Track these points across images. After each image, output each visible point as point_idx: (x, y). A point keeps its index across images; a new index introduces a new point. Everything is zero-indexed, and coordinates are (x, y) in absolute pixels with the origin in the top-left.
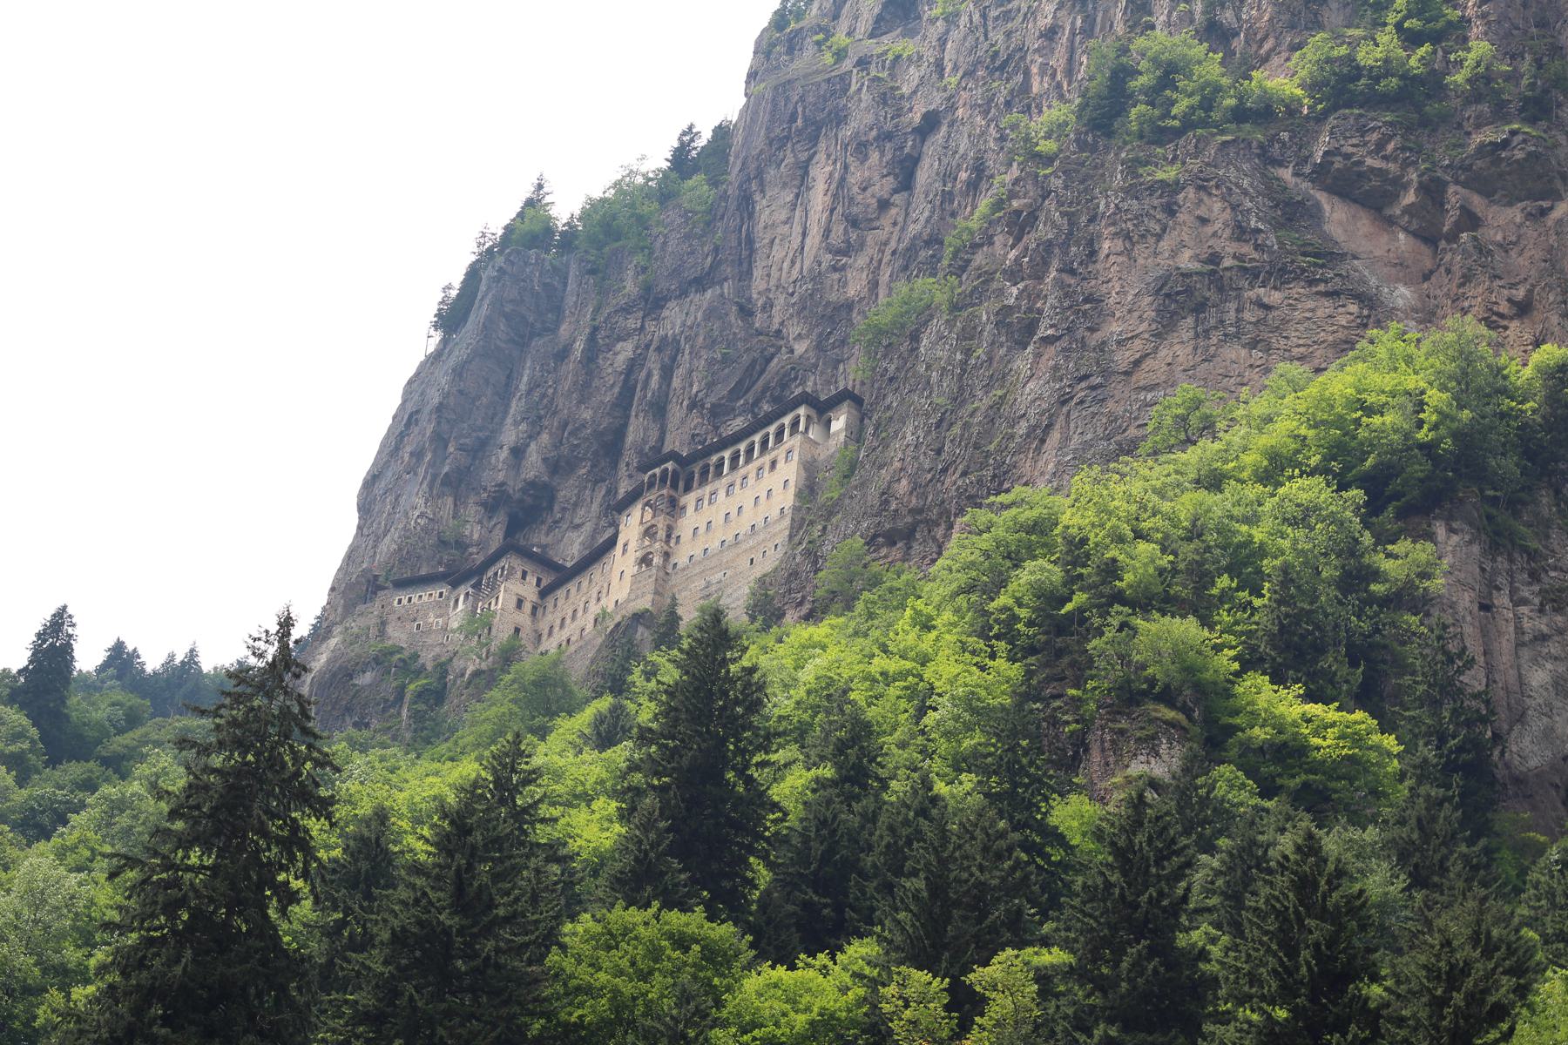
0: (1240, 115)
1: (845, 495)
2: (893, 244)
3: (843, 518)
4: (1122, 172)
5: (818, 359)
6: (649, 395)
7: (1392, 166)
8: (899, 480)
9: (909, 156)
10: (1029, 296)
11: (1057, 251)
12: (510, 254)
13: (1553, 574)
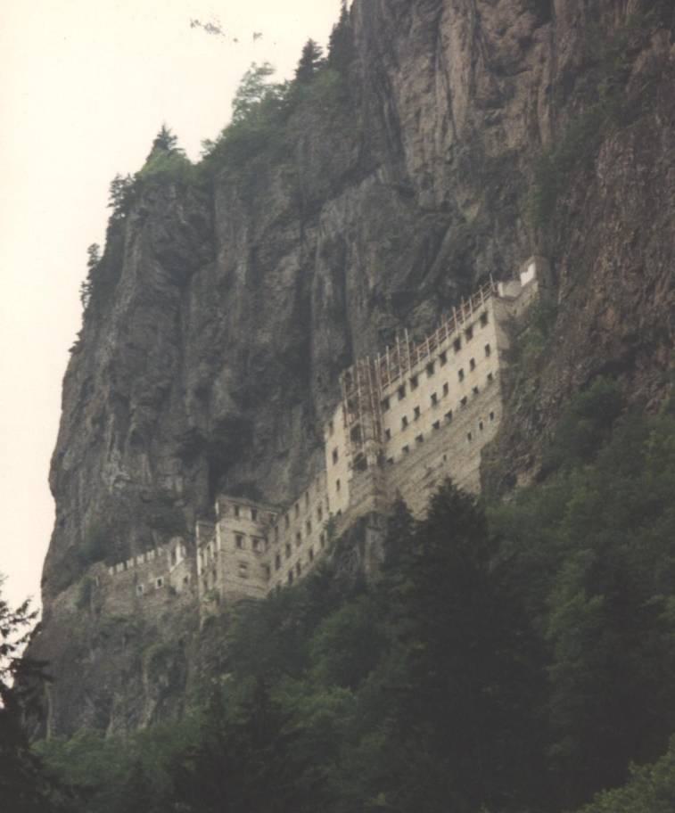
6: (326, 303)
8: (605, 312)
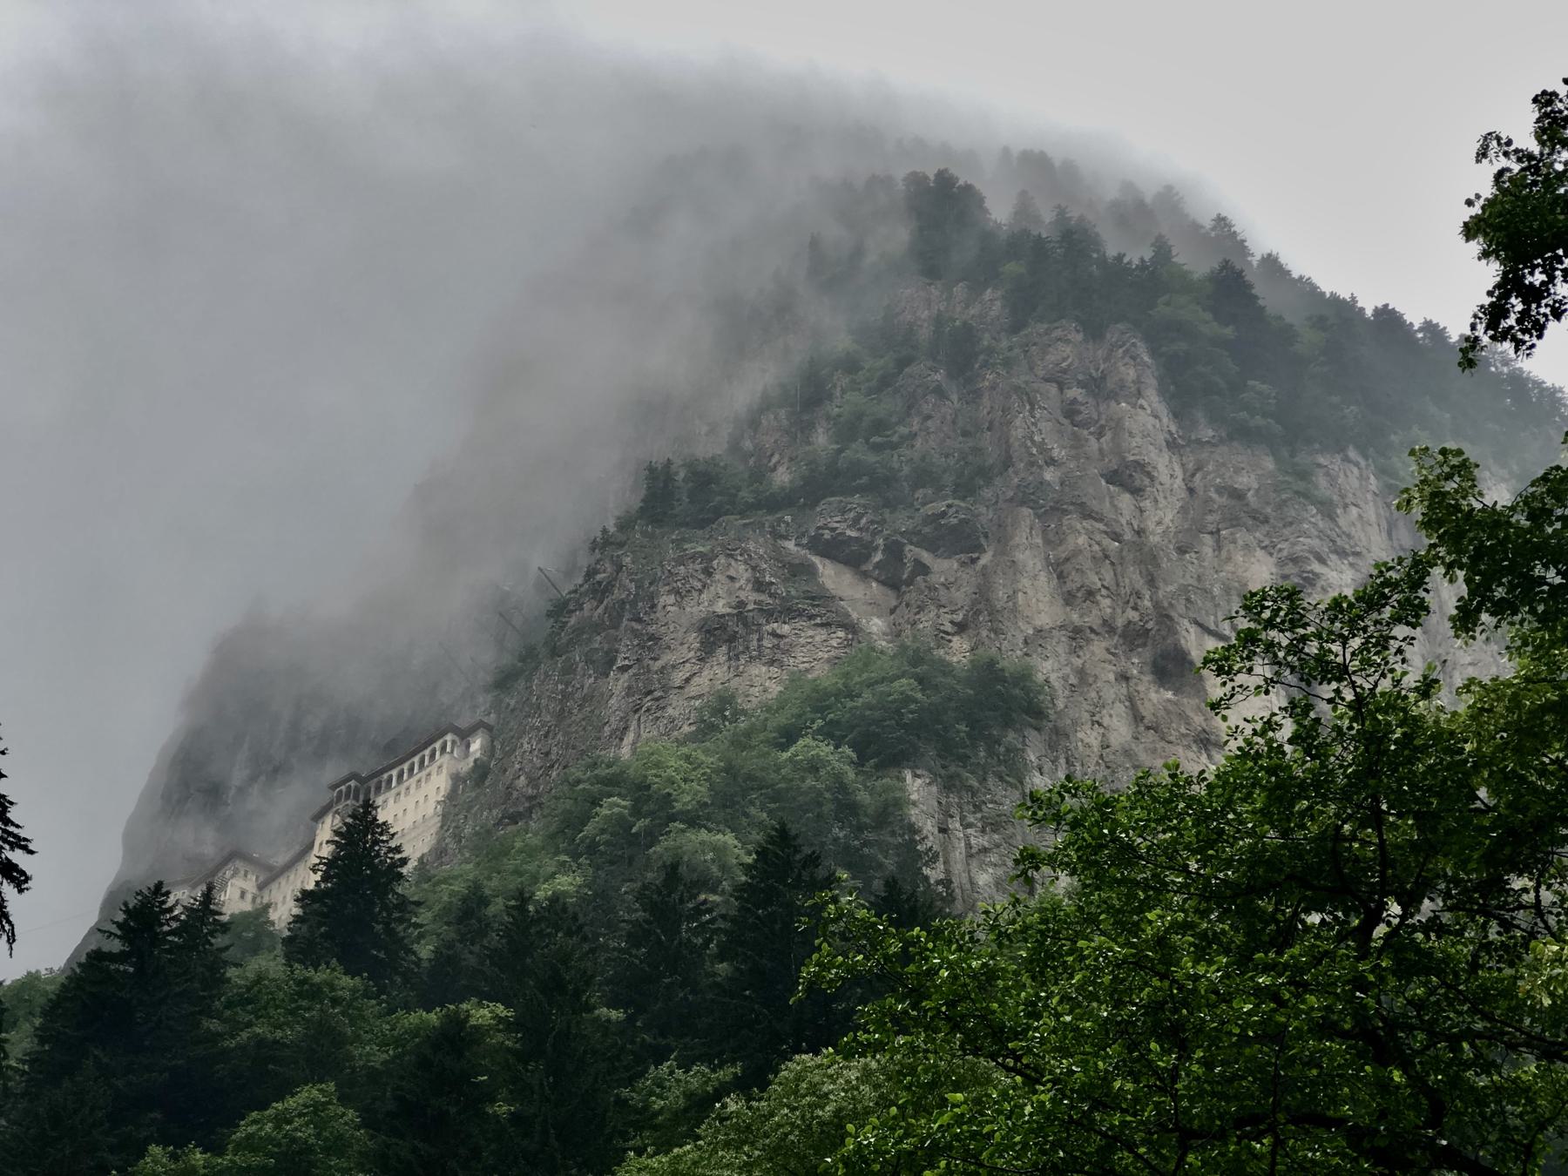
11: (628, 607)
13: (990, 806)
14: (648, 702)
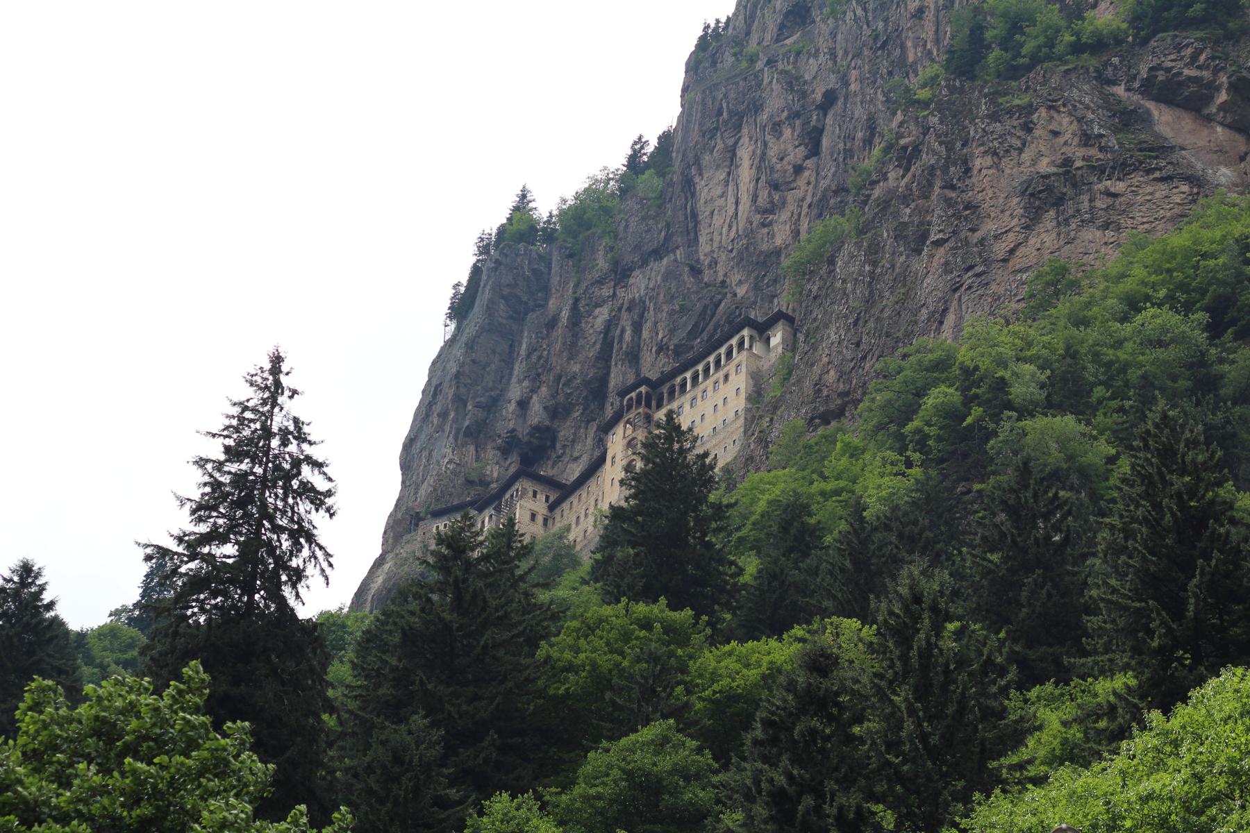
0: (1078, 48)
1: (785, 392)
2: (809, 200)
3: (785, 410)
4: (986, 103)
5: (756, 297)
6: (624, 346)
7: (1206, 74)
8: (828, 372)
9: (815, 128)
10: (920, 212)
11: (938, 173)
12: (503, 248)
14: (968, 279)
